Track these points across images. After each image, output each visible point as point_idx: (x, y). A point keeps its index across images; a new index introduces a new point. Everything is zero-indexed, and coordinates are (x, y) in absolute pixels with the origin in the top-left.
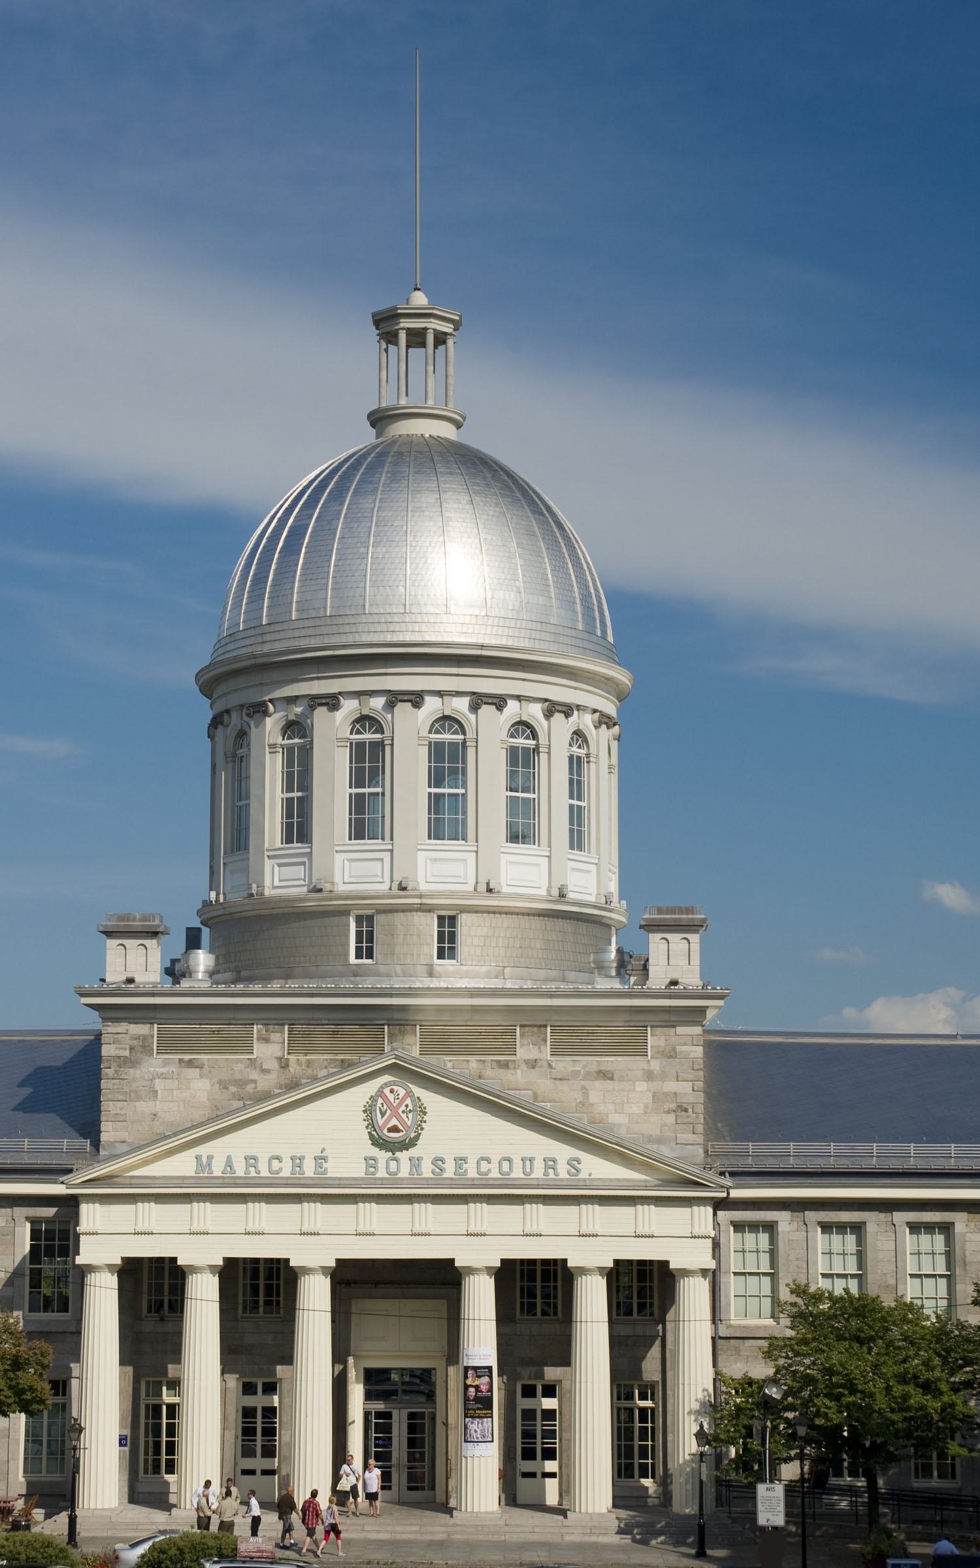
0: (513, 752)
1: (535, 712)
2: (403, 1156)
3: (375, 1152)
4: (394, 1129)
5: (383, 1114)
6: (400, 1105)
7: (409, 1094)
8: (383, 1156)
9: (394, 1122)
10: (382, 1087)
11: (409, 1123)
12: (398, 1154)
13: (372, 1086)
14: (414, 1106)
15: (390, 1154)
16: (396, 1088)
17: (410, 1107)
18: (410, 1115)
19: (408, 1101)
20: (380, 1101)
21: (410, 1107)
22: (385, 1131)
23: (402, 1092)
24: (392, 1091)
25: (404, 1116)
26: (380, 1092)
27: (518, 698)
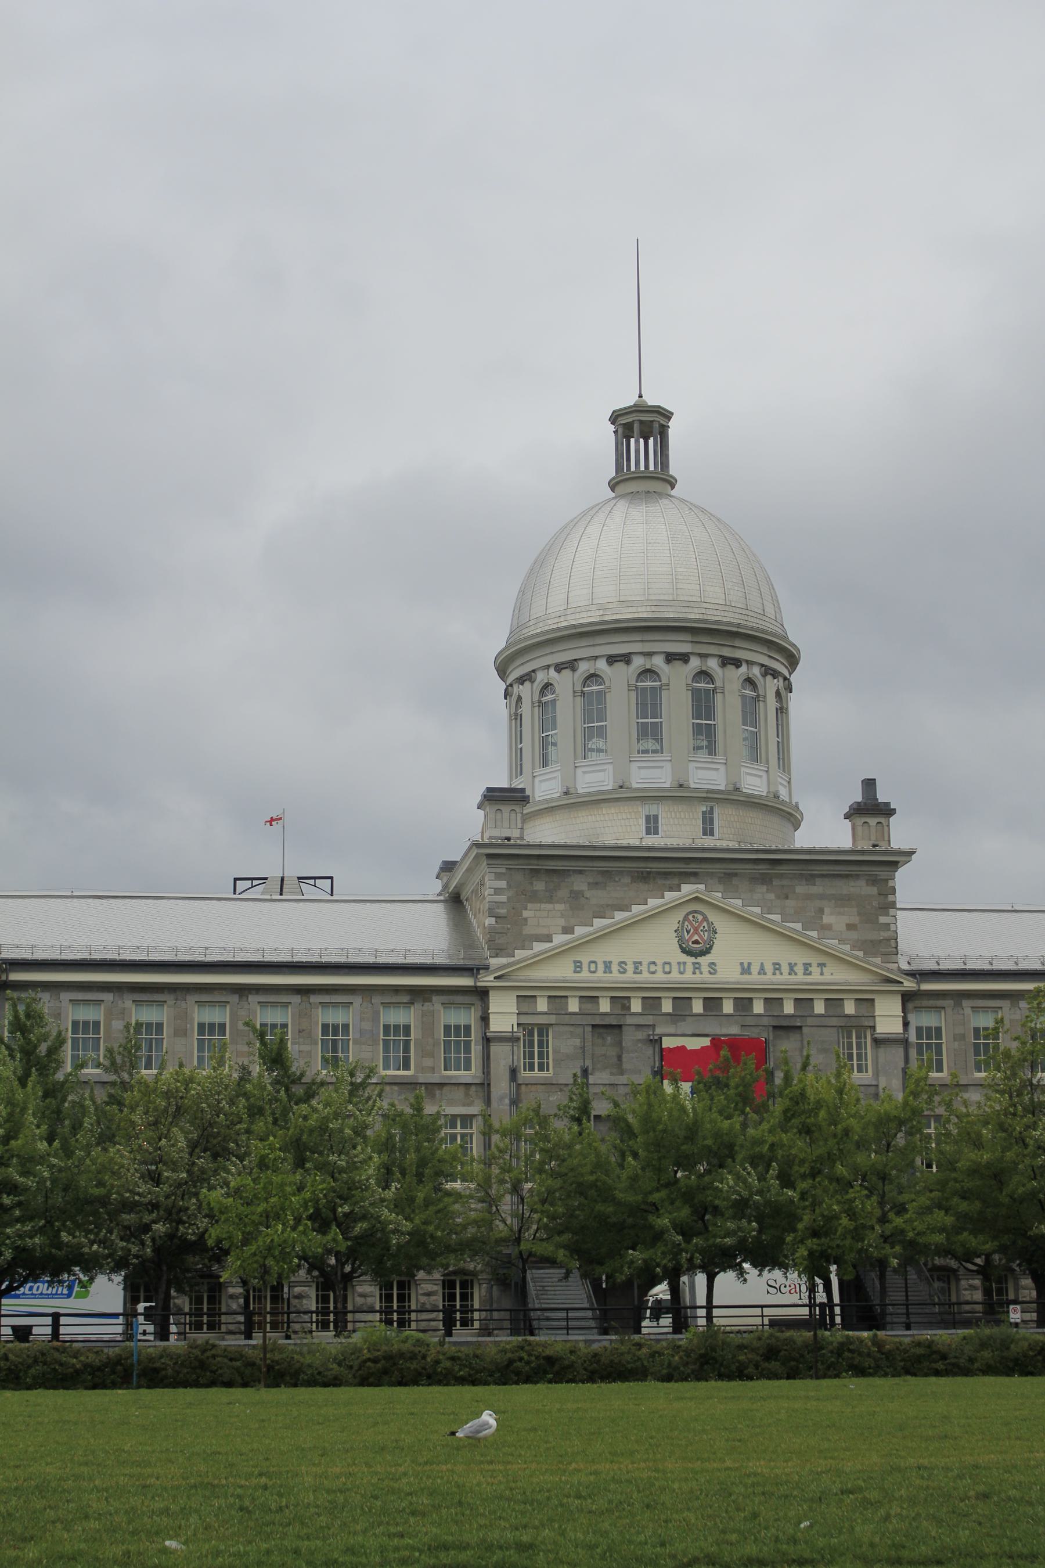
0: (744, 697)
1: (756, 671)
2: (704, 961)
3: (684, 958)
4: (696, 942)
5: (688, 932)
6: (699, 926)
7: (705, 919)
8: (690, 960)
9: (696, 937)
10: (687, 914)
11: (705, 938)
12: (699, 959)
13: (680, 915)
14: (709, 927)
15: (693, 959)
16: (696, 915)
17: (706, 928)
18: (706, 933)
19: (705, 924)
20: (686, 923)
21: (706, 928)
22: (690, 943)
23: (700, 918)
24: (694, 917)
25: (702, 933)
26: (686, 918)
27: (747, 661)
